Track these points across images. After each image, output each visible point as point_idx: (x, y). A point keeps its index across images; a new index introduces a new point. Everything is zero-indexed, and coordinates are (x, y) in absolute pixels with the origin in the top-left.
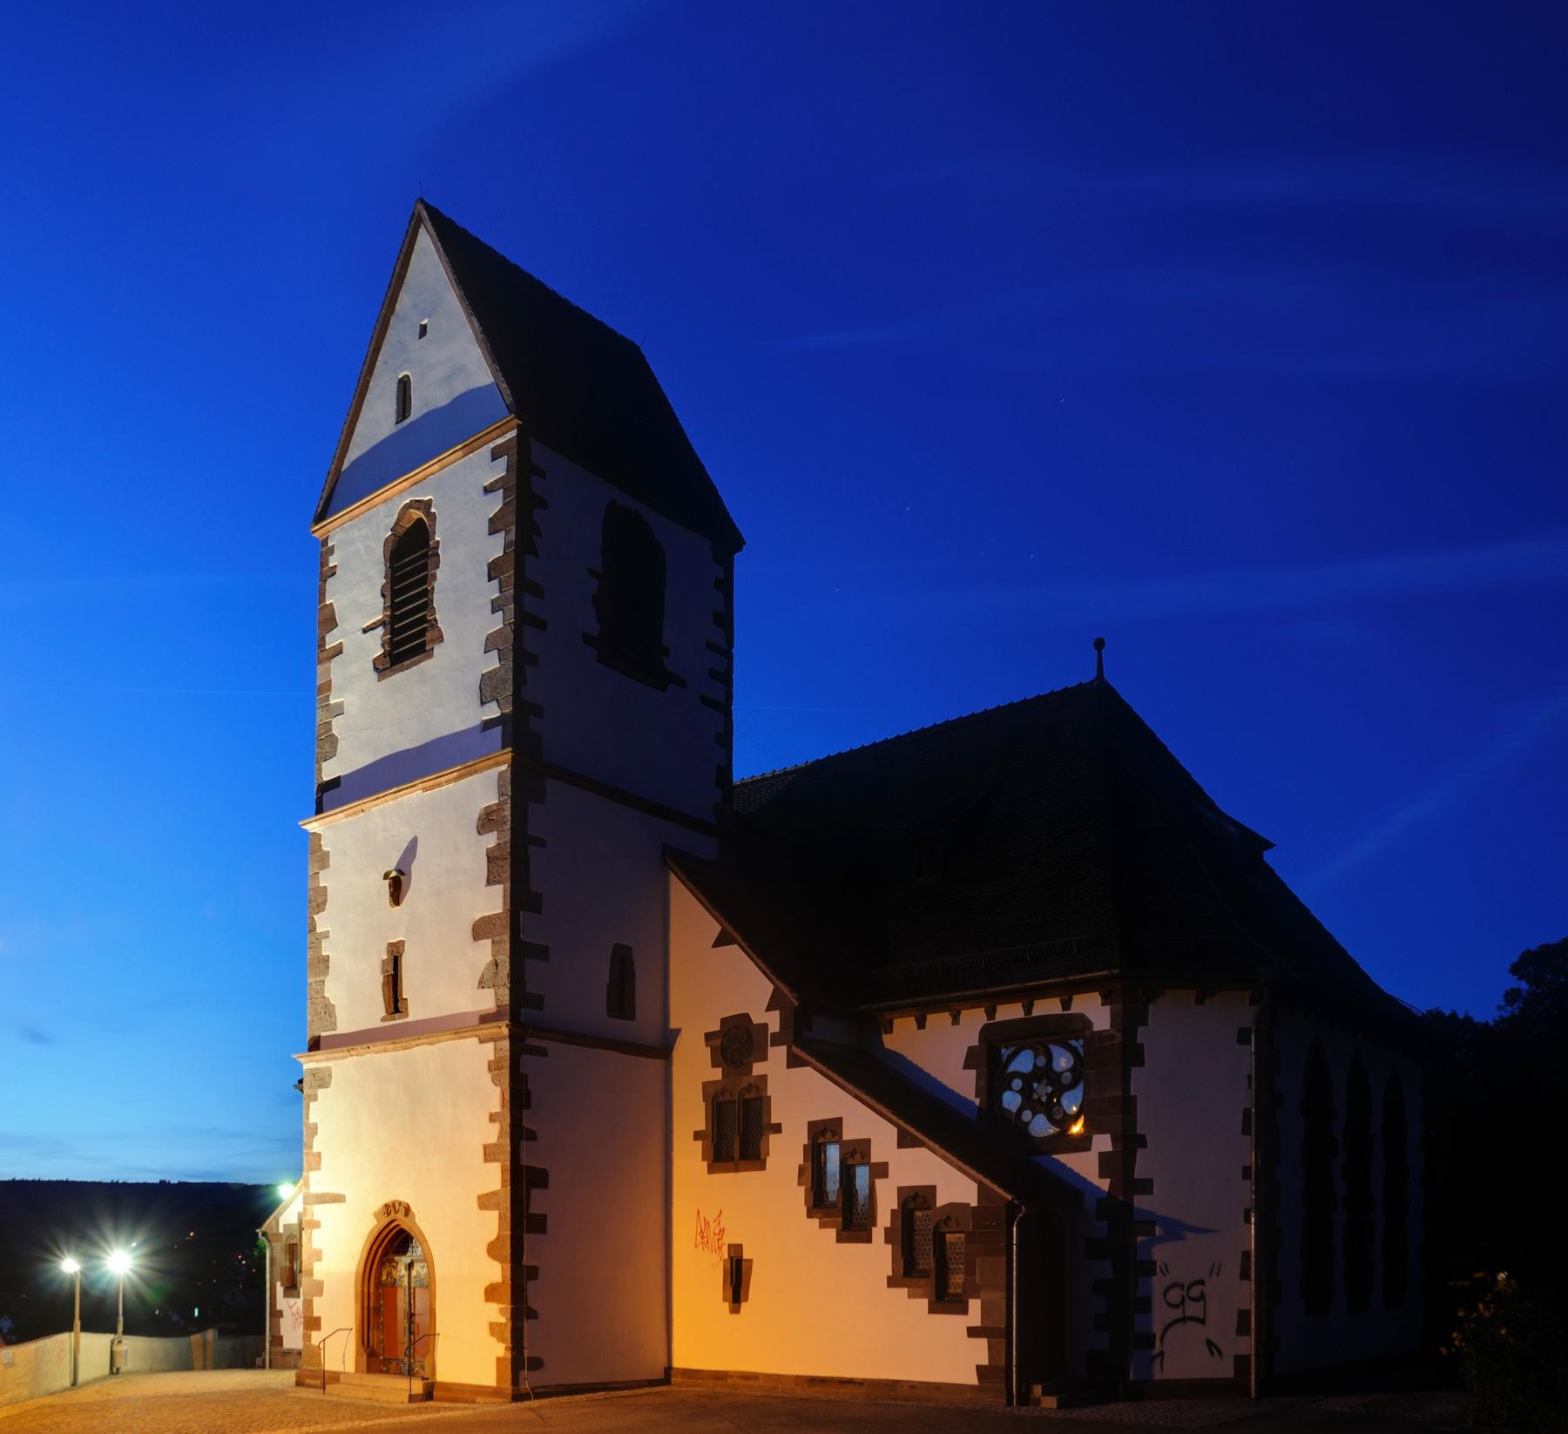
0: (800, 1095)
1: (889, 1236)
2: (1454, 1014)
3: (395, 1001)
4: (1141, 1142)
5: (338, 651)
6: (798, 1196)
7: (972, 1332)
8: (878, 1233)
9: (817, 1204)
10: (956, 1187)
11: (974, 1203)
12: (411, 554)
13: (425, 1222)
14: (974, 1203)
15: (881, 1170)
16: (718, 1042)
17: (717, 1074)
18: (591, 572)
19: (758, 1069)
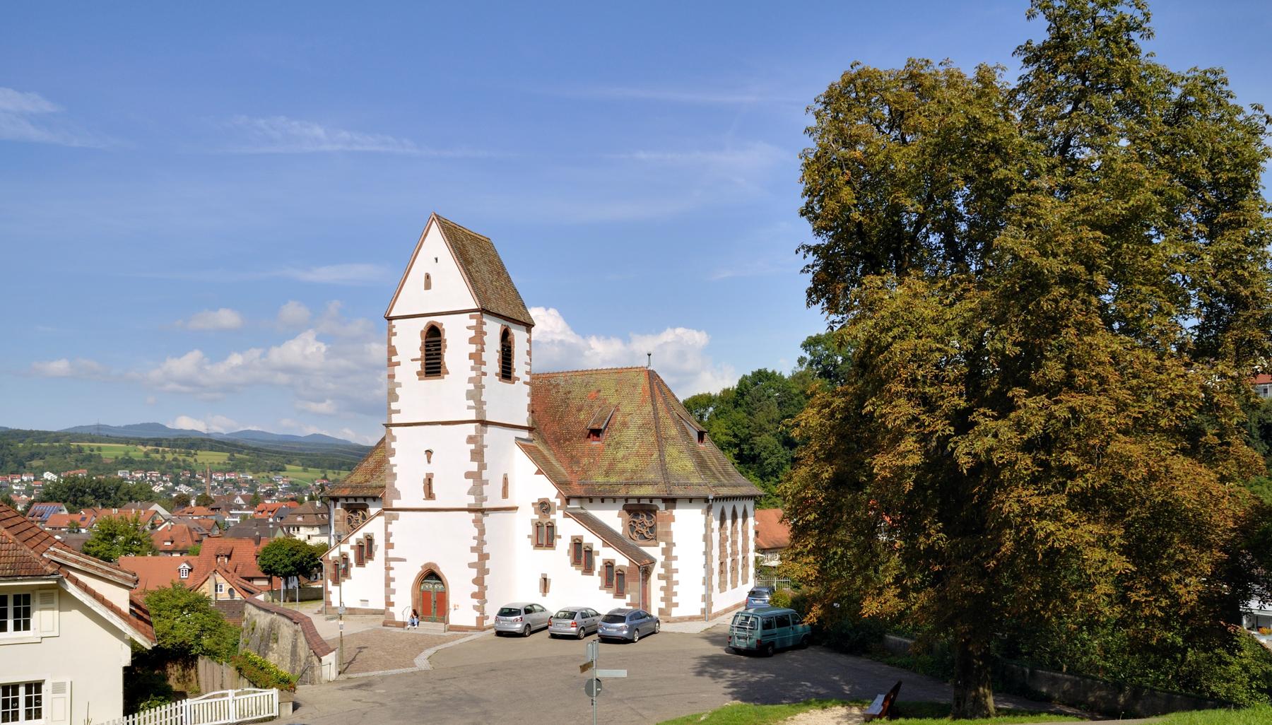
0: (567, 528)
1: (600, 574)
2: (774, 373)
3: (430, 495)
5: (398, 364)
6: (567, 560)
8: (596, 573)
9: (576, 561)
10: (621, 561)
12: (433, 337)
13: (444, 571)
15: (598, 553)
17: (537, 517)
19: (552, 517)
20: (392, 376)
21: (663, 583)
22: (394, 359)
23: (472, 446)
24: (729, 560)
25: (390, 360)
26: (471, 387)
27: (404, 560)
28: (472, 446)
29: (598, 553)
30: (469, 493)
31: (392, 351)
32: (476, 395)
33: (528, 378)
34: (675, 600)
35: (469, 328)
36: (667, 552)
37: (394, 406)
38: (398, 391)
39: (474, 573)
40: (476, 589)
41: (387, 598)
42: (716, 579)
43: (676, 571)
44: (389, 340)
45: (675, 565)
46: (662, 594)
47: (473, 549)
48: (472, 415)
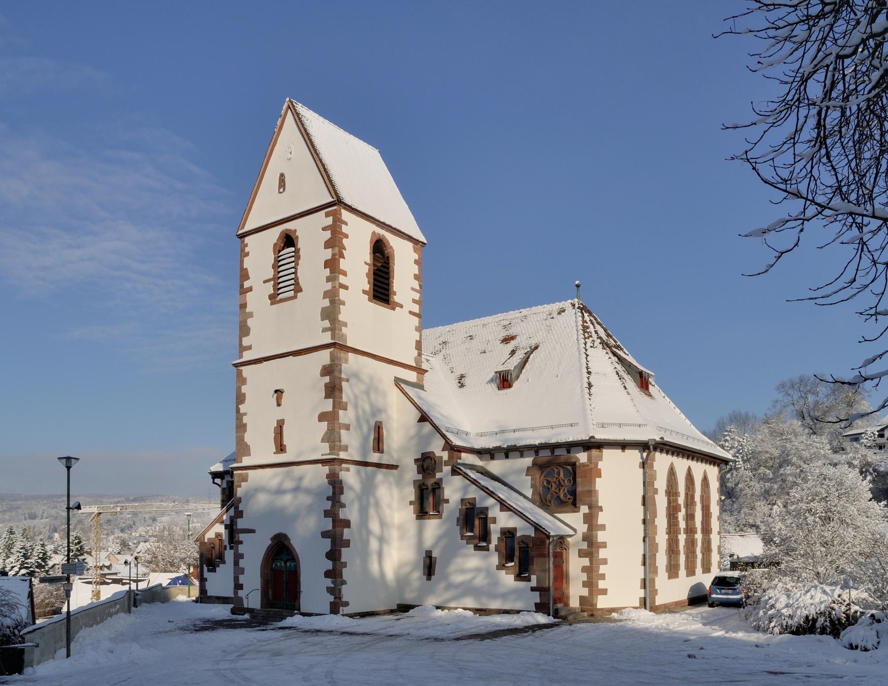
3: (281, 448)
4: (601, 509)
5: (250, 289)
7: (533, 589)
11: (533, 535)
13: (297, 543)
14: (533, 535)
16: (420, 463)
17: (420, 477)
18: (366, 263)
19: (438, 475)
20: (243, 306)
21: (586, 562)
22: (247, 284)
23: (327, 379)
24: (682, 538)
25: (242, 286)
26: (326, 303)
27: (253, 531)
28: (327, 379)
29: (494, 521)
30: (323, 441)
31: (244, 275)
32: (331, 314)
33: (416, 308)
34: (601, 584)
35: (324, 229)
36: (590, 519)
37: (246, 341)
38: (250, 322)
39: (327, 544)
40: (329, 565)
41: (236, 579)
42: (662, 560)
43: (604, 545)
44: (242, 262)
45: (601, 536)
46: (584, 577)
47: (327, 514)
48: (327, 339)
